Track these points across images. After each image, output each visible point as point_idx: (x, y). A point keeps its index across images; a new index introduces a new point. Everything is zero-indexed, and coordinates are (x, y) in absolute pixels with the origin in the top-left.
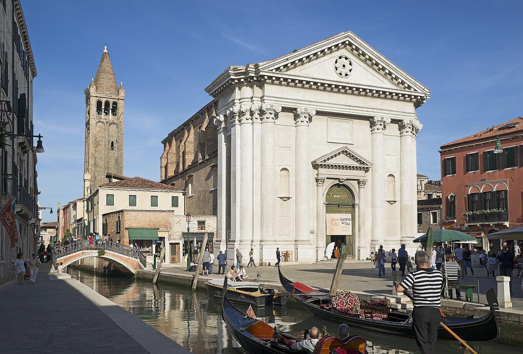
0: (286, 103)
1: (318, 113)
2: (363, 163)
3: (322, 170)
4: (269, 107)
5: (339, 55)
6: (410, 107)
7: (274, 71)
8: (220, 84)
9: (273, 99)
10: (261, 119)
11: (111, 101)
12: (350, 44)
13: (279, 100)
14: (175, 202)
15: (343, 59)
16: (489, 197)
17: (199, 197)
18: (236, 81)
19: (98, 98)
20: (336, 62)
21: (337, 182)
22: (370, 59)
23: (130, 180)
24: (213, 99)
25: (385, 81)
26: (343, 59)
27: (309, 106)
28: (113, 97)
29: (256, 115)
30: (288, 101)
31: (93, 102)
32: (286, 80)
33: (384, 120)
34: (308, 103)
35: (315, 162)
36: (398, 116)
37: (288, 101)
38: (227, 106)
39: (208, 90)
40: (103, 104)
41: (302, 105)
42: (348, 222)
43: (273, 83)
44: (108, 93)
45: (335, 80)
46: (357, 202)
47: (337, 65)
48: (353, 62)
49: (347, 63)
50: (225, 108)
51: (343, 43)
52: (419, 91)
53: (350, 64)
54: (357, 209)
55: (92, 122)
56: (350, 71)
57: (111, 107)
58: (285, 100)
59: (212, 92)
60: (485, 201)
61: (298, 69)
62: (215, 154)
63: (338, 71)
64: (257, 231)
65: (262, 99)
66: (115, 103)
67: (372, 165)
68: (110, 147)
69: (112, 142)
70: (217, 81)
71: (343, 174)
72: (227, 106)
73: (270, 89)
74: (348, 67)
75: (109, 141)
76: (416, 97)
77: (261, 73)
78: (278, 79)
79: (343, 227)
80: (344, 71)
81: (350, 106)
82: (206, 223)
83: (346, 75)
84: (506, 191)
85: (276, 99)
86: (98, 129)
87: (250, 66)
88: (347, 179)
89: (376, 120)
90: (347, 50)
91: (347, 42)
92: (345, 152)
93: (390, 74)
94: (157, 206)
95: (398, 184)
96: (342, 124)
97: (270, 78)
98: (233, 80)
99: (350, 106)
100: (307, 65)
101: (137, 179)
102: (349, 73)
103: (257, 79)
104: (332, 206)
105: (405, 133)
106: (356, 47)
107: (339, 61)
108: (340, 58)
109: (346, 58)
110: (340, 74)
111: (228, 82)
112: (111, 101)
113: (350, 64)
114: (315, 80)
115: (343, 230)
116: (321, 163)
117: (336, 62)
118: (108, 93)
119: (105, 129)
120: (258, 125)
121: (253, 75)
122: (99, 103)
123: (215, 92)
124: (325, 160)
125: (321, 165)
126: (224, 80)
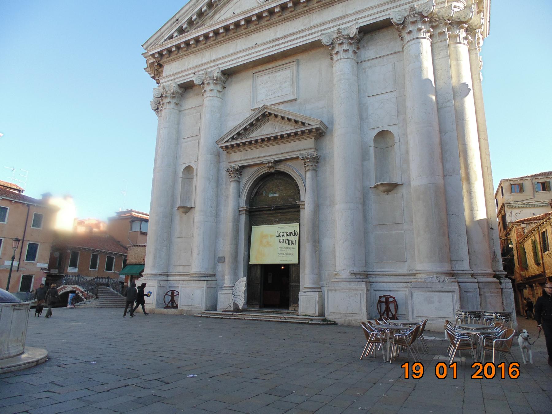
0: (186, 77)
2: (303, 124)
33: (345, 33)
42: (292, 238)
46: (302, 199)
58: (183, 74)
71: (268, 154)
78: (169, 51)
79: (281, 249)
81: (278, 39)
85: (173, 78)
97: (161, 54)
99: (278, 39)
114: (213, 29)
115: (281, 255)
116: (226, 144)
124: (233, 138)
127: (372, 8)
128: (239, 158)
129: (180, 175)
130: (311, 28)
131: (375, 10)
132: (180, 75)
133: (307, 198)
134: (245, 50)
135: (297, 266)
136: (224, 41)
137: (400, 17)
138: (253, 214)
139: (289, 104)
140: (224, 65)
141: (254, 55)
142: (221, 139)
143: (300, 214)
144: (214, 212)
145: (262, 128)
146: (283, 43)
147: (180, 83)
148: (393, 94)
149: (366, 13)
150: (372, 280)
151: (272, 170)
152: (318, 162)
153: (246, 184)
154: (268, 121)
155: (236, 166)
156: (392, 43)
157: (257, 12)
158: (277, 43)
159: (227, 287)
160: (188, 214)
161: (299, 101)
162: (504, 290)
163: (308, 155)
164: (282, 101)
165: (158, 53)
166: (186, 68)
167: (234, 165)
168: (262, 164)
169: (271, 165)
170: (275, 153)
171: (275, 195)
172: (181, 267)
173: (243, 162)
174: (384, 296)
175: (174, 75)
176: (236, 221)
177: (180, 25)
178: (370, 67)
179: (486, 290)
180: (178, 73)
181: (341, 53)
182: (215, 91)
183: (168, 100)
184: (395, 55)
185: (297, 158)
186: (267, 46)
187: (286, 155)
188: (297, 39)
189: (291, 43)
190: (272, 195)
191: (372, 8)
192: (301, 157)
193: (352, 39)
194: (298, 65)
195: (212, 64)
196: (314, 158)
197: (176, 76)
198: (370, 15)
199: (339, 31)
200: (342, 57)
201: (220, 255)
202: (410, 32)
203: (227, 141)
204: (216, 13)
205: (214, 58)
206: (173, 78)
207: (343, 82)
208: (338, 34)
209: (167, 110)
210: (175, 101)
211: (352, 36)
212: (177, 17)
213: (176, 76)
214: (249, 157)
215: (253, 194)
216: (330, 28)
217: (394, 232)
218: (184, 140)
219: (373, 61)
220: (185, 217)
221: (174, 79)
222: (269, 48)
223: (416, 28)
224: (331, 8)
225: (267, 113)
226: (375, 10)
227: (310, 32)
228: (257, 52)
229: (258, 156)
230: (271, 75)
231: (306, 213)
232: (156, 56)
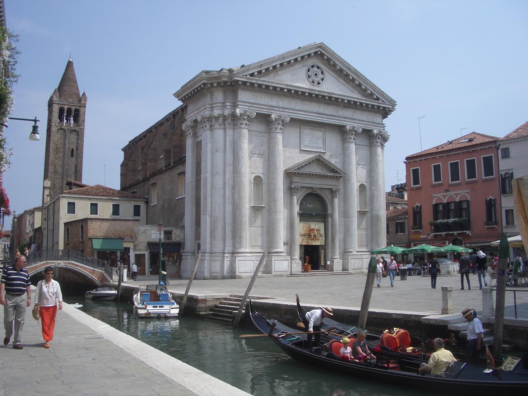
0: (260, 109)
1: (292, 120)
2: (336, 172)
3: (296, 179)
5: (311, 65)
7: (248, 76)
8: (190, 88)
9: (247, 104)
10: (234, 125)
11: (73, 108)
12: (322, 55)
14: (137, 211)
15: (315, 69)
16: (452, 207)
17: (163, 206)
18: (209, 85)
19: (60, 106)
20: (309, 71)
21: (309, 191)
22: (341, 70)
23: (92, 188)
24: (180, 103)
25: (355, 92)
26: (315, 69)
27: (283, 113)
28: (76, 104)
29: (229, 121)
31: (56, 109)
32: (260, 86)
34: (281, 110)
35: (289, 169)
37: (262, 107)
38: (198, 111)
39: (177, 95)
40: (66, 111)
41: (276, 112)
44: (70, 100)
45: (308, 87)
46: (329, 211)
47: (310, 73)
48: (325, 72)
49: (319, 72)
50: (196, 112)
51: (316, 53)
54: (330, 219)
55: (54, 129)
56: (322, 80)
57: (73, 115)
58: (259, 106)
59: (182, 96)
60: (449, 211)
61: (271, 76)
62: (182, 161)
63: (310, 80)
64: (229, 242)
65: (235, 106)
66: (77, 111)
67: (345, 174)
68: (70, 154)
69: (73, 149)
70: (188, 86)
71: (316, 183)
72: (198, 111)
73: (243, 96)
74: (320, 76)
75: (69, 148)
76: (384, 108)
78: (252, 84)
80: (316, 80)
81: (323, 114)
82: (173, 233)
83: (319, 84)
84: (468, 202)
85: (250, 105)
86: (58, 136)
87: (224, 71)
88: (321, 189)
91: (319, 53)
92: (319, 161)
93: (360, 85)
94: (118, 215)
95: (368, 194)
96: (315, 132)
97: (244, 83)
98: (205, 84)
99: (323, 114)
100: (280, 72)
101: (99, 187)
102: (321, 82)
103: (231, 83)
104: (304, 216)
105: (375, 144)
106: (327, 57)
107: (311, 69)
108: (312, 67)
109: (318, 68)
110: (313, 82)
111: (200, 86)
112: (73, 108)
113: (322, 73)
114: (289, 88)
117: (309, 71)
118: (70, 100)
119: (65, 136)
120: (230, 132)
121: (226, 80)
122: (61, 110)
123: (185, 97)
125: (295, 173)
126: (196, 84)
127: (365, 121)
129: (252, 181)
132: (257, 106)
135: (324, 247)
136: (289, 96)
141: (309, 117)
142: (294, 168)
157: (317, 93)
158: (321, 116)
165: (242, 81)
166: (259, 102)
175: (251, 103)
180: (255, 104)
186: (315, 115)
189: (328, 120)
191: (365, 121)
195: (281, 110)
197: (253, 105)
206: (250, 105)
212: (262, 63)
221: (251, 107)
227: (338, 119)
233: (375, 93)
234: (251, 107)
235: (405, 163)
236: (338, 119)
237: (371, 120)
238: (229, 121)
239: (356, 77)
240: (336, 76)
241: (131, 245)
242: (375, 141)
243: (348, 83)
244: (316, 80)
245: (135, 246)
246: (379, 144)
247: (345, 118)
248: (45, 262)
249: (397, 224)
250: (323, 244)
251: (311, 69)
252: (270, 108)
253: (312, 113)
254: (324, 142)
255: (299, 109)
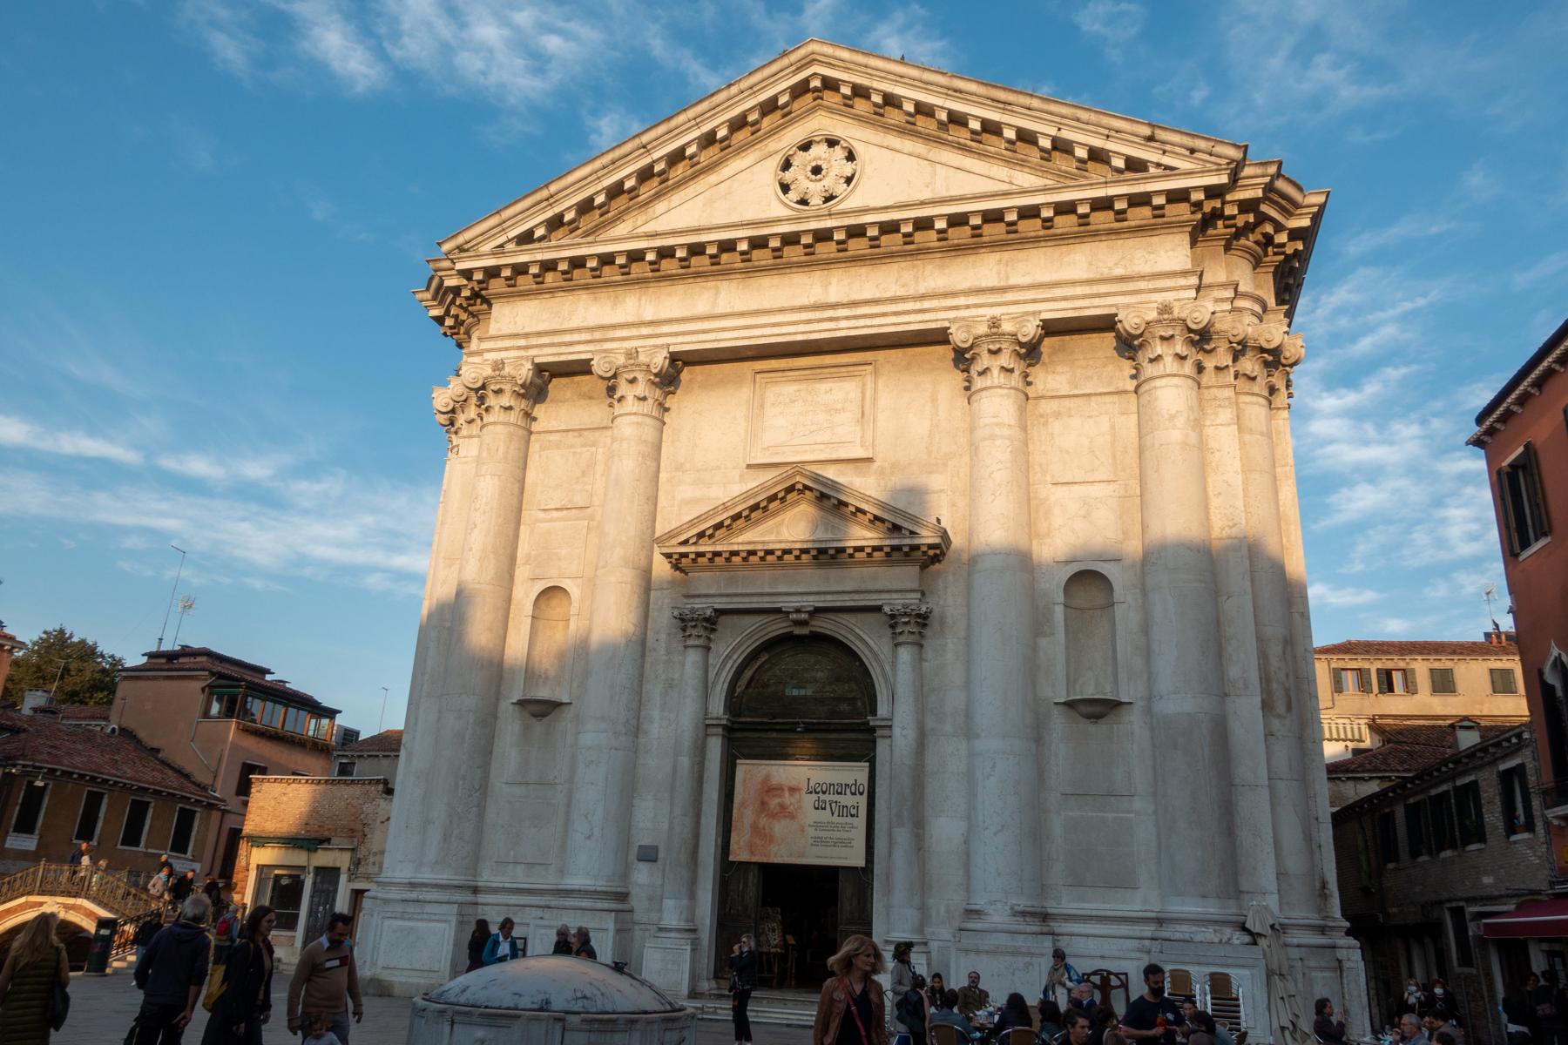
4: (488, 371)
6: (1172, 252)
7: (511, 246)
12: (830, 85)
13: (534, 341)
20: (787, 165)
21: (778, 628)
26: (819, 151)
30: (567, 338)
34: (645, 331)
36: (1097, 301)
37: (567, 338)
43: (514, 294)
46: (882, 710)
47: (788, 176)
48: (859, 149)
51: (800, 90)
52: (1183, 165)
53: (851, 157)
56: (849, 180)
58: (556, 339)
63: (793, 195)
77: (460, 266)
85: (522, 342)
89: (959, 337)
90: (830, 110)
91: (816, 83)
96: (823, 387)
100: (660, 207)
105: (1149, 370)
107: (800, 159)
108: (805, 147)
109: (832, 143)
110: (803, 202)
113: (851, 157)
114: (658, 243)
116: (683, 549)
117: (787, 165)
124: (701, 535)
127: (1074, 283)
128: (712, 589)
129: (528, 608)
130: (923, 297)
131: (1079, 290)
133: (898, 710)
134: (742, 314)
137: (1137, 320)
138: (739, 735)
139: (852, 466)
140: (680, 339)
143: (874, 749)
144: (634, 722)
145: (779, 519)
146: (847, 318)
147: (545, 360)
148: (1112, 487)
149: (1058, 292)
150: (1058, 930)
151: (804, 631)
152: (925, 625)
153: (728, 657)
154: (795, 503)
155: (704, 606)
156: (1110, 368)
159: (670, 930)
160: (545, 720)
161: (876, 465)
162: (1346, 965)
163: (904, 606)
164: (834, 456)
167: (698, 604)
168: (778, 611)
169: (804, 616)
170: (815, 589)
171: (803, 692)
172: (520, 869)
173: (724, 600)
174: (1095, 973)
175: (526, 335)
176: (700, 752)
177: (557, 210)
178: (1057, 415)
179: (1313, 963)
180: (539, 334)
181: (995, 372)
182: (650, 401)
183: (506, 400)
184: (1115, 398)
185: (878, 609)
187: (846, 597)
188: (884, 315)
189: (869, 322)
190: (795, 692)
191: (1074, 283)
192: (887, 609)
193: (1021, 344)
194: (876, 373)
196: (919, 616)
198: (1065, 299)
199: (995, 323)
200: (996, 382)
201: (646, 842)
202: (1158, 358)
203: (685, 542)
204: (658, 196)
205: (648, 315)
206: (522, 342)
207: (998, 443)
208: (990, 327)
209: (499, 428)
210: (523, 404)
211: (1024, 340)
213: (534, 341)
214: (740, 591)
215: (743, 682)
216: (968, 307)
217: (1110, 816)
218: (542, 515)
219: (1067, 402)
220: (538, 727)
221: (526, 348)
222: (809, 322)
223: (1171, 351)
224: (971, 259)
225: (799, 486)
226: (1079, 290)
227: (918, 305)
228: (774, 325)
229: (767, 590)
230: (803, 386)
231: (896, 747)
232: (478, 276)
233: (1110, 146)
234: (526, 348)
235: (1477, 442)
236: (918, 305)
237: (1119, 271)
238: (472, 412)
239: (994, 116)
240: (919, 147)
241: (342, 860)
242: (1145, 364)
243: (982, 155)
244: (815, 189)
245: (357, 863)
246: (1169, 364)
247: (954, 294)
248: (22, 900)
249: (1507, 777)
250: (861, 863)
251: (800, 159)
252: (598, 335)
253: (782, 310)
254: (864, 416)
255: (729, 310)
